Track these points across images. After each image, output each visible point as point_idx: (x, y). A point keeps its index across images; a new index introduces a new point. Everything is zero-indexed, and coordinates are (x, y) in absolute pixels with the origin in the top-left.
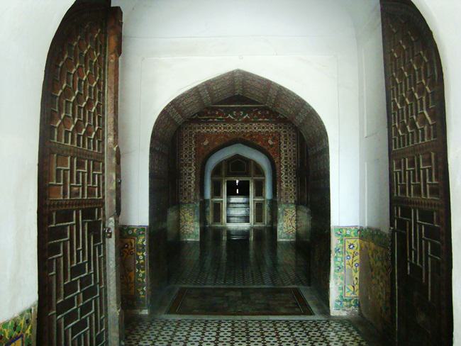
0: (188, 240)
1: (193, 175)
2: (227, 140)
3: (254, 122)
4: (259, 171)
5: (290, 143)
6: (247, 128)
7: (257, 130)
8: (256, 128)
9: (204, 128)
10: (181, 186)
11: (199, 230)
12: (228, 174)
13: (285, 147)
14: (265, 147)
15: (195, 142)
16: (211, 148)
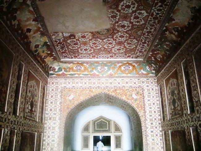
1: (57, 129)
2: (92, 95)
3: (116, 77)
4: (117, 129)
5: (153, 97)
6: (111, 83)
7: (120, 85)
9: (69, 83)
10: (44, 140)
12: (95, 131)
13: (149, 100)
14: (130, 102)
15: (61, 96)
16: (76, 103)
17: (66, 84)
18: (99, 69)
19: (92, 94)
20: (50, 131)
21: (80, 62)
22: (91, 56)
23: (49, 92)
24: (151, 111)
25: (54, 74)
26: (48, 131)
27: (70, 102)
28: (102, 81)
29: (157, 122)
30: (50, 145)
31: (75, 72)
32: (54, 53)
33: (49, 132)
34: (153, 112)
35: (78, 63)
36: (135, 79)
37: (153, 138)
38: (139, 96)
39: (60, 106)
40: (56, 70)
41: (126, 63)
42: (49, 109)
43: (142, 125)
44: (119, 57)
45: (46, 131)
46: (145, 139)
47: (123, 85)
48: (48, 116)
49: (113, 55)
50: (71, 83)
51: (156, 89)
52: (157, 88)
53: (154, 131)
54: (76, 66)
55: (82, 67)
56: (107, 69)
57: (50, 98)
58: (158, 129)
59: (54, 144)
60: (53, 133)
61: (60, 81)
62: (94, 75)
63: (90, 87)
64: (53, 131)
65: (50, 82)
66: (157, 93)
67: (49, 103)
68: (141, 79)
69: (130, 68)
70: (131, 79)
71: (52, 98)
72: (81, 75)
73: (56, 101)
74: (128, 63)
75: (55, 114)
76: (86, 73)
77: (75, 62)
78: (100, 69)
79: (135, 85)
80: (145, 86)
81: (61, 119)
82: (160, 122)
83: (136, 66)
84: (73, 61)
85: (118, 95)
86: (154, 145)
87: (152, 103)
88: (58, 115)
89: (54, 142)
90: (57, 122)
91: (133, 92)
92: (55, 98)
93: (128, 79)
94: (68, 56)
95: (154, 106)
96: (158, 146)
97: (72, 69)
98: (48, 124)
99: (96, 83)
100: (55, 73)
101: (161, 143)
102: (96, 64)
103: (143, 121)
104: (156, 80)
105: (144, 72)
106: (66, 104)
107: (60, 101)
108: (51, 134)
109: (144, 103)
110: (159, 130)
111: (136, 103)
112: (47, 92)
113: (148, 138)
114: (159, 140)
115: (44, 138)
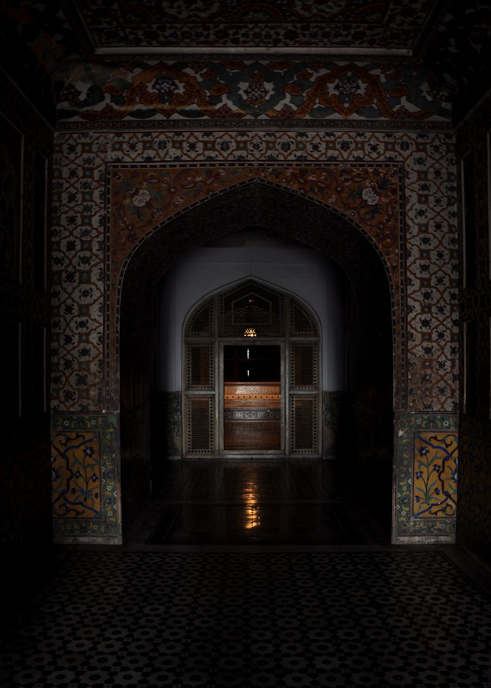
0: (84, 540)
5: (438, 201)
6: (286, 146)
8: (316, 144)
9: (133, 147)
11: (118, 506)
13: (421, 213)
16: (160, 218)
17: (121, 149)
18: (241, 92)
19: (216, 185)
20: (72, 319)
21: (170, 63)
22: (212, 32)
23: (61, 181)
24: (428, 252)
25: (73, 114)
26: (65, 319)
27: (138, 217)
28: (253, 137)
29: (445, 290)
30: (76, 366)
31: (151, 103)
32: (61, 14)
33: (68, 324)
34: (434, 256)
35: (162, 66)
36: (376, 134)
37: (425, 344)
38: (386, 196)
39: (101, 229)
40: (82, 97)
41: (346, 69)
42: (63, 245)
43: (392, 300)
44: (319, 37)
45: (57, 319)
46: (401, 347)
47: (330, 153)
48: (63, 268)
49: (299, 25)
50: (140, 146)
51: (450, 174)
52: (454, 170)
53: (435, 323)
54: (154, 80)
55: (177, 82)
56: (272, 93)
57: (65, 205)
58: (448, 314)
59: (88, 362)
60: (81, 327)
61: (98, 139)
62: (224, 117)
63: (210, 159)
64: (84, 319)
65: (61, 145)
66: (452, 189)
67: (64, 221)
68: (398, 135)
69: (358, 87)
70: (361, 131)
71: (72, 205)
72: (176, 116)
73: (89, 214)
74: (352, 67)
75: (86, 260)
76: (194, 107)
77: (153, 63)
78: (246, 92)
79: (374, 155)
80: (409, 158)
81: (108, 276)
82: (456, 291)
83: (383, 79)
84: (143, 55)
85: (312, 190)
86: (430, 367)
87: (432, 223)
88: (96, 265)
89: (87, 358)
90: (94, 287)
91: (367, 182)
92: (85, 203)
93: (351, 134)
94: (121, 33)
95: (439, 234)
96: (441, 372)
97: (139, 90)
98: (63, 296)
99: (233, 145)
100: (75, 108)
101: (453, 361)
102: (231, 72)
103: (397, 287)
104: (454, 140)
105: (411, 108)
106: (124, 222)
107: (103, 212)
108: (75, 331)
109: (403, 221)
110: (449, 320)
111: (374, 222)
112: (54, 181)
113: (410, 344)
114: (447, 351)
115: (54, 345)
